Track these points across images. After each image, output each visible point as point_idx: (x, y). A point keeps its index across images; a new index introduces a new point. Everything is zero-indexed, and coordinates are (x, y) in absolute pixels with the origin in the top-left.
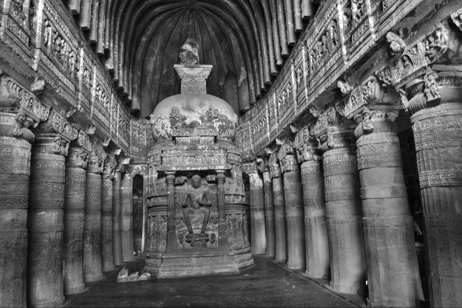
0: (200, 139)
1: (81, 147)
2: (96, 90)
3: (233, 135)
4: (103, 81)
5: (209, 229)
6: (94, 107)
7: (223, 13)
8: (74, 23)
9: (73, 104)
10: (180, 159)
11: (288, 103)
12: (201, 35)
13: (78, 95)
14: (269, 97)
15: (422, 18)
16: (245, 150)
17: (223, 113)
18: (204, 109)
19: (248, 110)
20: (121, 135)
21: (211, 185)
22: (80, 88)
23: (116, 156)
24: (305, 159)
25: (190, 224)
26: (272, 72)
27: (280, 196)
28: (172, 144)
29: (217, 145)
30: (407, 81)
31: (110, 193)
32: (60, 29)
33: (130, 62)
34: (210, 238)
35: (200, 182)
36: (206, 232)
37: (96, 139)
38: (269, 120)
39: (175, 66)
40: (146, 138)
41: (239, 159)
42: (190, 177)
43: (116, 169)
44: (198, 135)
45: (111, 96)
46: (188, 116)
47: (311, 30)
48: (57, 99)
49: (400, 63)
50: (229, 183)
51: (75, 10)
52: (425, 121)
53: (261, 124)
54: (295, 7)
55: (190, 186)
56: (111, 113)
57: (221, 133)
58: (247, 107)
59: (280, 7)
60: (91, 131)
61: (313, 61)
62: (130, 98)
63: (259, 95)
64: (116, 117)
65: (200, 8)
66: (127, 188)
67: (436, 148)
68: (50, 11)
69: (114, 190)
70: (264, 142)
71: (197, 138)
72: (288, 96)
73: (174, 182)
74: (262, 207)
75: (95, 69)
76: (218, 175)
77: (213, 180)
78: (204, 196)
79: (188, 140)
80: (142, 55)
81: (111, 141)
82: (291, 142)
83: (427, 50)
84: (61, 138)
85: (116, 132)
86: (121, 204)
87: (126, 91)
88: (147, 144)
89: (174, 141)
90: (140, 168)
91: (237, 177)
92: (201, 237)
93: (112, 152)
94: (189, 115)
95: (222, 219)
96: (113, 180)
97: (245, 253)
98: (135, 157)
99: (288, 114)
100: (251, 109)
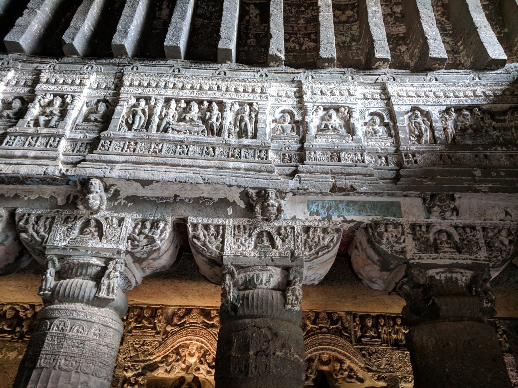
15: (149, 195)
30: (77, 253)
49: (79, 224)
52: (79, 322)
67: (77, 372)
83: (134, 232)
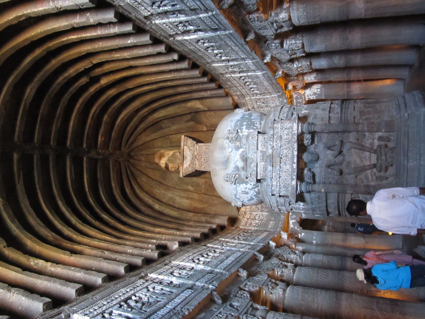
0: (261, 151)
1: (260, 289)
2: (198, 263)
3: (258, 114)
4: (190, 254)
5: (372, 144)
6: (216, 267)
7: (132, 124)
8: (119, 281)
9: (206, 295)
10: (283, 175)
11: (221, 45)
12: (155, 148)
13: (198, 286)
14: (217, 73)
16: (278, 104)
17: (233, 123)
18: (227, 145)
19: (233, 99)
20: (254, 239)
21: (316, 140)
22: (191, 282)
23: (277, 247)
24: (287, 19)
25: (364, 166)
26: (187, 66)
27: (333, 59)
28: (265, 184)
29: (268, 132)
31: (319, 257)
32: (119, 300)
33: (177, 223)
34: (382, 143)
35: (312, 153)
36: (375, 147)
37: (254, 269)
38: (243, 72)
39: (181, 175)
40: (260, 213)
41: (287, 107)
42: (306, 164)
43: (292, 248)
44: (256, 153)
45: (209, 247)
46: (235, 163)
47: (130, 10)
48: (198, 314)
50: (315, 118)
51: (102, 279)
53: (248, 83)
54: (109, 32)
55: (317, 165)
56: (228, 248)
57: (255, 128)
58: (230, 100)
59: (116, 56)
60: (244, 274)
61: (165, 6)
62: (214, 226)
63: (216, 85)
64: (233, 243)
65: (127, 147)
66: (314, 237)
68: (95, 310)
69: (316, 253)
70: (269, 79)
71: (259, 154)
72: (212, 44)
73: (310, 183)
74: (345, 85)
75: (175, 263)
76: (304, 131)
77: (310, 137)
78: (329, 148)
79: (261, 165)
80: (172, 210)
81: (258, 251)
82: (268, 42)
84: (245, 314)
85: (249, 245)
86: (332, 245)
87: (206, 230)
88: (267, 212)
89: (262, 181)
90: (294, 221)
91: (308, 110)
92: (381, 153)
93: (272, 251)
94: (233, 163)
95: (360, 128)
96: (304, 252)
97: (405, 100)
98: (280, 226)
99: (233, 44)
100: (231, 96)
